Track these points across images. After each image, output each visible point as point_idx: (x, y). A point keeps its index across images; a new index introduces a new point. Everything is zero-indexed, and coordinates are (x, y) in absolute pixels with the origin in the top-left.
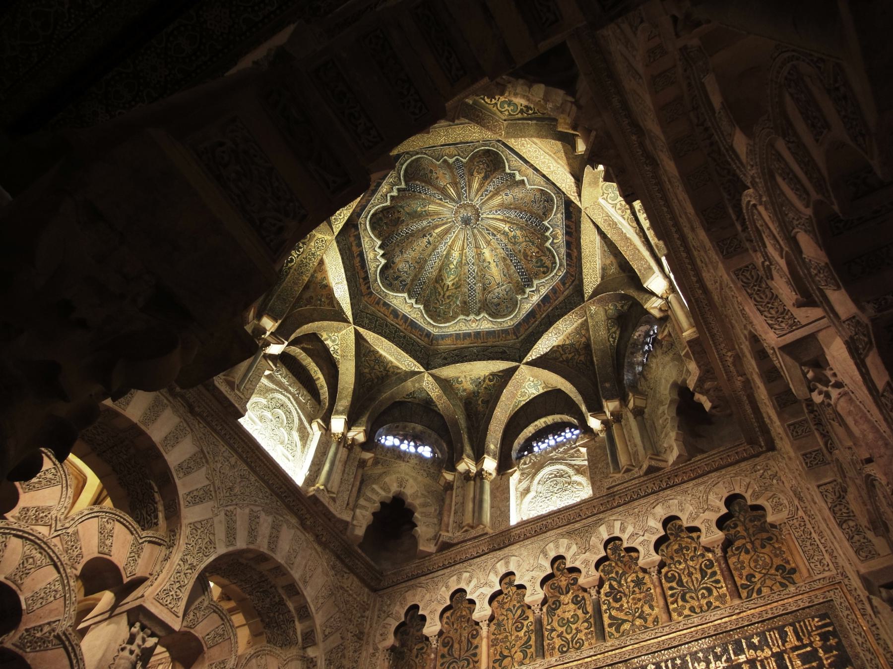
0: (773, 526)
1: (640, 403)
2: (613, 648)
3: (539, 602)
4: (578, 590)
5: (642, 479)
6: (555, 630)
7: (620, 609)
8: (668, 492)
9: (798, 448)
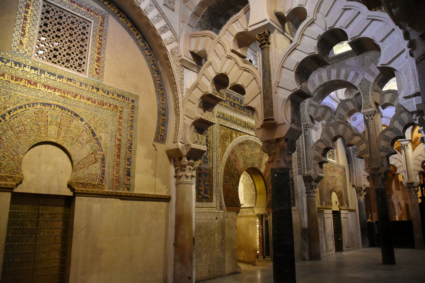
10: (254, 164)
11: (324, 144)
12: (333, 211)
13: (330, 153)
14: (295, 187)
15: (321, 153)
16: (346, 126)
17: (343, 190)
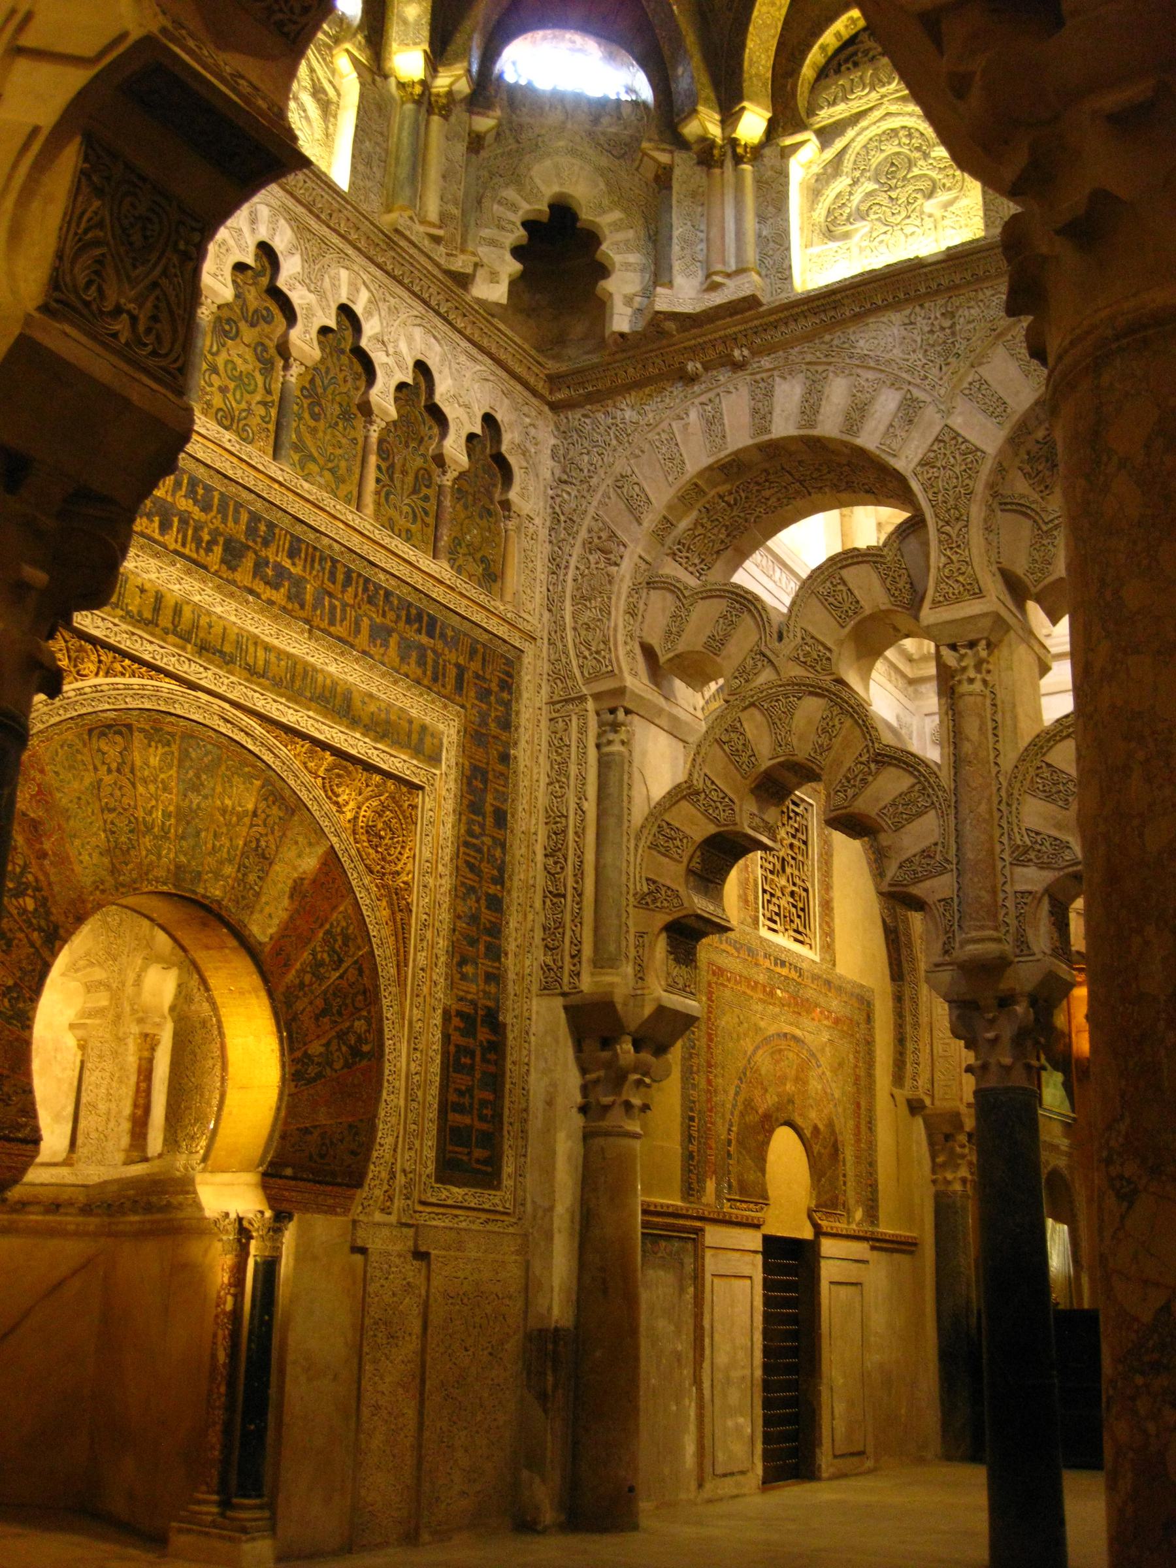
0: (506, 505)
1: (489, 139)
2: (311, 498)
3: (220, 301)
4: (271, 339)
5: (436, 272)
6: (218, 374)
7: (313, 431)
8: (438, 321)
9: (670, 507)
10: (199, 874)
11: (705, 813)
12: (767, 1239)
13: (783, 903)
14: (509, 1066)
15: (681, 869)
16: (836, 710)
17: (851, 1124)
